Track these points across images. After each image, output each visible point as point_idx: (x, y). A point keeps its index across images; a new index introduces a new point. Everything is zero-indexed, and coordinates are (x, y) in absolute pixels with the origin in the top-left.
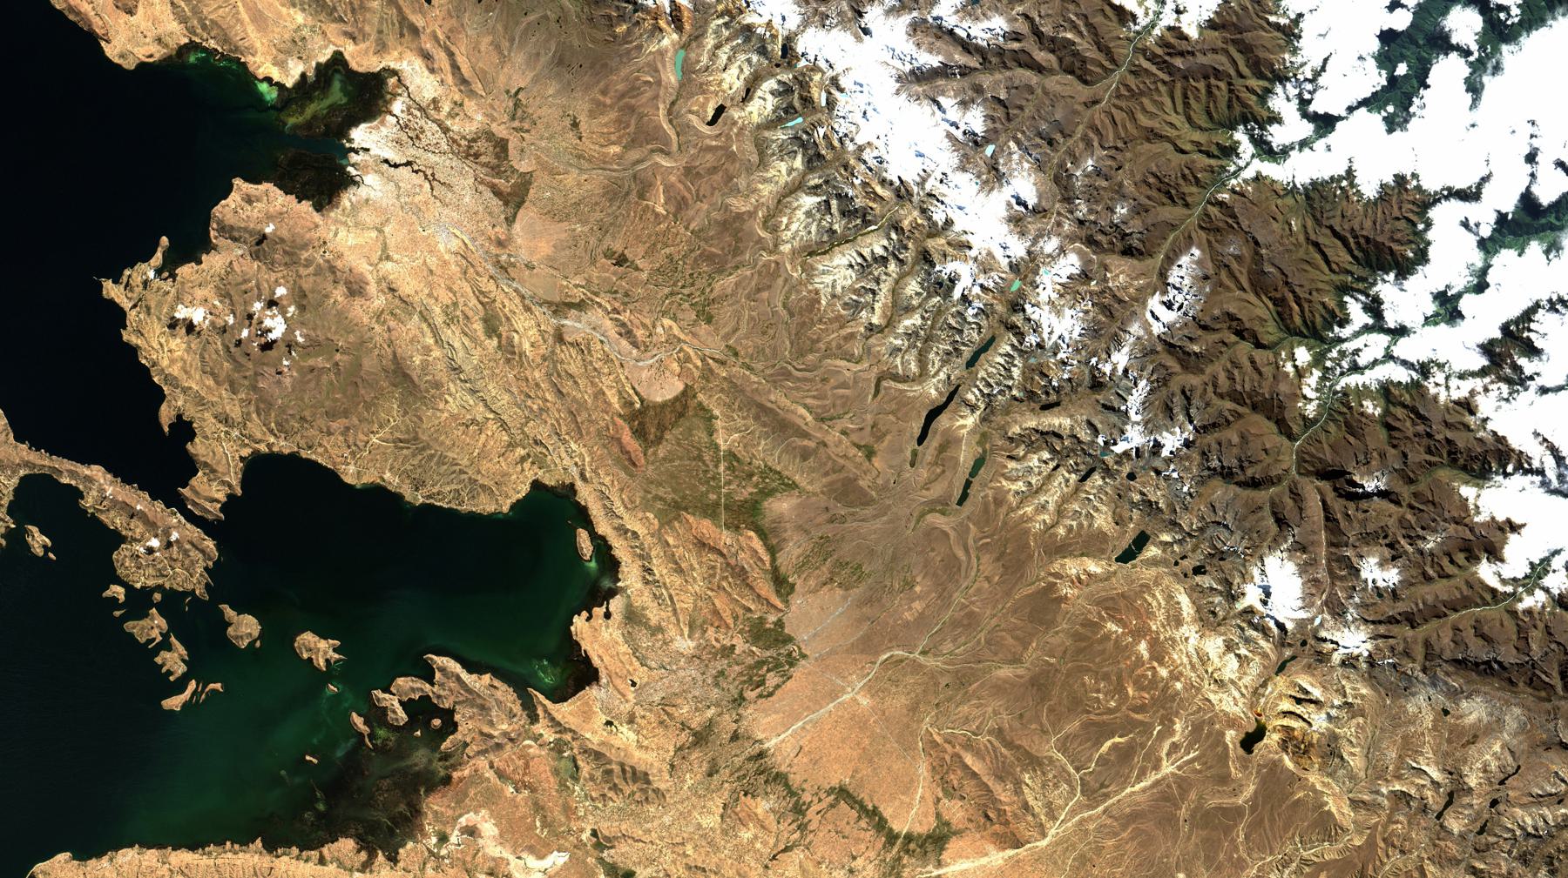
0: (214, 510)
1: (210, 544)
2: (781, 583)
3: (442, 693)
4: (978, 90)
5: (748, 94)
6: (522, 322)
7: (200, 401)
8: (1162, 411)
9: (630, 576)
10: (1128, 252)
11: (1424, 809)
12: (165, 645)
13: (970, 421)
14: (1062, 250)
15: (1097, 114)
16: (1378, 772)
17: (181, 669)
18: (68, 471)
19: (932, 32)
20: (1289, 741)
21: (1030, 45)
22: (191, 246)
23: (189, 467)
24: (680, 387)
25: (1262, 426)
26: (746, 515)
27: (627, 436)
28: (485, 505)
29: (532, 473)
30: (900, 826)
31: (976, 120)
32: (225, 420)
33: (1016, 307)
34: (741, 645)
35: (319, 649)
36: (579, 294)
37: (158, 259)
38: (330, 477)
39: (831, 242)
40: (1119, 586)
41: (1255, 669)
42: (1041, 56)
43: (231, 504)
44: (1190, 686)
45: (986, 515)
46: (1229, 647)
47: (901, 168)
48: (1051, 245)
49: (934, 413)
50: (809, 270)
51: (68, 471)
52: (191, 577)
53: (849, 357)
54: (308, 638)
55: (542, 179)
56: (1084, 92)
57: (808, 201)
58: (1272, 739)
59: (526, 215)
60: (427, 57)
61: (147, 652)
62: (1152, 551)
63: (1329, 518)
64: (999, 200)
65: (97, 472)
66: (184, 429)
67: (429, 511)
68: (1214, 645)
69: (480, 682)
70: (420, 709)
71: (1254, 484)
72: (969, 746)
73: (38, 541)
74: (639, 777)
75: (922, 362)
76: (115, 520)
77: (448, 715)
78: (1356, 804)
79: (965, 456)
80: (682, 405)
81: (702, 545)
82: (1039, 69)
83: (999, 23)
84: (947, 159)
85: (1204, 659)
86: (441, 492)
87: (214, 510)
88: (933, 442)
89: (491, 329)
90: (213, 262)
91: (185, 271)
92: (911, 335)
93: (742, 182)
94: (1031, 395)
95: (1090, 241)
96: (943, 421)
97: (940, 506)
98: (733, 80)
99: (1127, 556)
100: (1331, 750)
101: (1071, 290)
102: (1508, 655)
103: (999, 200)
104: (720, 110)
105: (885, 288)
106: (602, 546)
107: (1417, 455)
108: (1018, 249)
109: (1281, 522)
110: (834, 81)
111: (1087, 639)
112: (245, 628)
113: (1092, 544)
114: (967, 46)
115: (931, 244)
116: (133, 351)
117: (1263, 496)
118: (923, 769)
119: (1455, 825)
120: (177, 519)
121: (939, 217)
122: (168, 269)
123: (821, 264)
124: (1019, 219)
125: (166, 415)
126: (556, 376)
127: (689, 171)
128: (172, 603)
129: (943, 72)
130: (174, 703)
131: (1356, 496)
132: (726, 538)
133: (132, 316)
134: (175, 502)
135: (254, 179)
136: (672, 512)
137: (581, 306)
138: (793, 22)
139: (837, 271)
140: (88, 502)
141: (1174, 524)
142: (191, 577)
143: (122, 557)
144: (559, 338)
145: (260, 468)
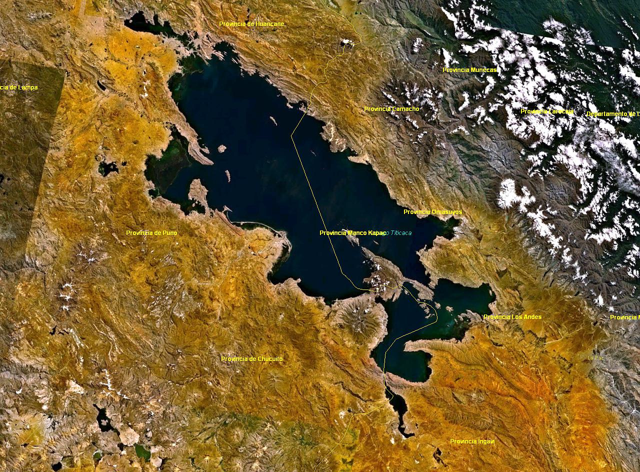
0: (434, 288)
1: (433, 293)
2: (521, 299)
3: (468, 316)
4: (553, 222)
5: (518, 222)
6: (481, 258)
7: (432, 271)
8: (582, 273)
9: (498, 298)
10: (577, 247)
11: (621, 334)
12: (426, 308)
13: (552, 274)
14: (567, 247)
15: (571, 226)
16: (614, 328)
17: (428, 312)
18: (411, 281)
19: (545, 213)
20: (601, 323)
21: (560, 215)
22: (430, 246)
23: (430, 280)
24: (505, 268)
25: (597, 275)
26: (516, 288)
27: (497, 275)
28: (475, 287)
29: (482, 281)
30: (539, 336)
31: (553, 227)
32: (435, 273)
33: (560, 256)
34: (515, 308)
35: (450, 309)
36: (490, 254)
37: (425, 248)
38: (451, 282)
39: (531, 246)
40: (575, 300)
41: (597, 313)
42: (562, 217)
43: (436, 286)
44: (586, 315)
45: (554, 289)
46: (593, 310)
47: (543, 234)
48: (565, 247)
49: (546, 273)
50: (527, 250)
51: (411, 281)
52: (430, 298)
53: (533, 264)
54: (448, 307)
55: (484, 235)
56: (569, 222)
57: (527, 239)
58: (598, 324)
59: (482, 241)
60: (466, 217)
61: (423, 309)
62: (580, 294)
63: (607, 289)
64: (558, 240)
65: (416, 281)
66: (429, 275)
67: (467, 287)
68: (590, 309)
69: (474, 314)
70: (465, 318)
71: (596, 284)
72: (550, 324)
73: (406, 292)
74: (499, 329)
75: (545, 265)
76: (418, 289)
77: (469, 319)
78: (610, 333)
79: (551, 279)
80: (505, 271)
81: (509, 293)
82: (562, 219)
83: (556, 212)
84: (550, 233)
85: (588, 311)
86: (468, 284)
87: (434, 288)
88: (546, 277)
89: (476, 259)
90: (434, 248)
91: (429, 250)
92: (543, 260)
93: (517, 237)
94: (561, 270)
95: (571, 245)
96: (547, 274)
97: (547, 287)
98: (516, 220)
99: (576, 295)
100: (607, 326)
101: (568, 254)
102: (634, 310)
103: (558, 240)
104: (514, 225)
105: (539, 253)
106: (493, 292)
107: (619, 279)
108: (560, 247)
109: (600, 290)
110: (533, 220)
111: (570, 307)
112: (438, 306)
113: (570, 293)
114: (552, 215)
115: (547, 246)
116: (421, 262)
117: (597, 286)
118: (543, 328)
119: (625, 337)
120: (428, 289)
121: (549, 242)
122: (426, 250)
123: (529, 249)
124: (560, 242)
125: (426, 272)
126: (486, 266)
127: (508, 235)
128: (427, 301)
129: (548, 219)
130: (427, 317)
131: (611, 286)
132: (513, 292)
133: (421, 257)
134: (427, 286)
135: (440, 236)
136: (504, 288)
137: (491, 256)
138: (526, 211)
139: (532, 250)
140: (414, 286)
141: (584, 290)
142: (430, 298)
143: (420, 295)
144: (487, 260)
145: (440, 280)
